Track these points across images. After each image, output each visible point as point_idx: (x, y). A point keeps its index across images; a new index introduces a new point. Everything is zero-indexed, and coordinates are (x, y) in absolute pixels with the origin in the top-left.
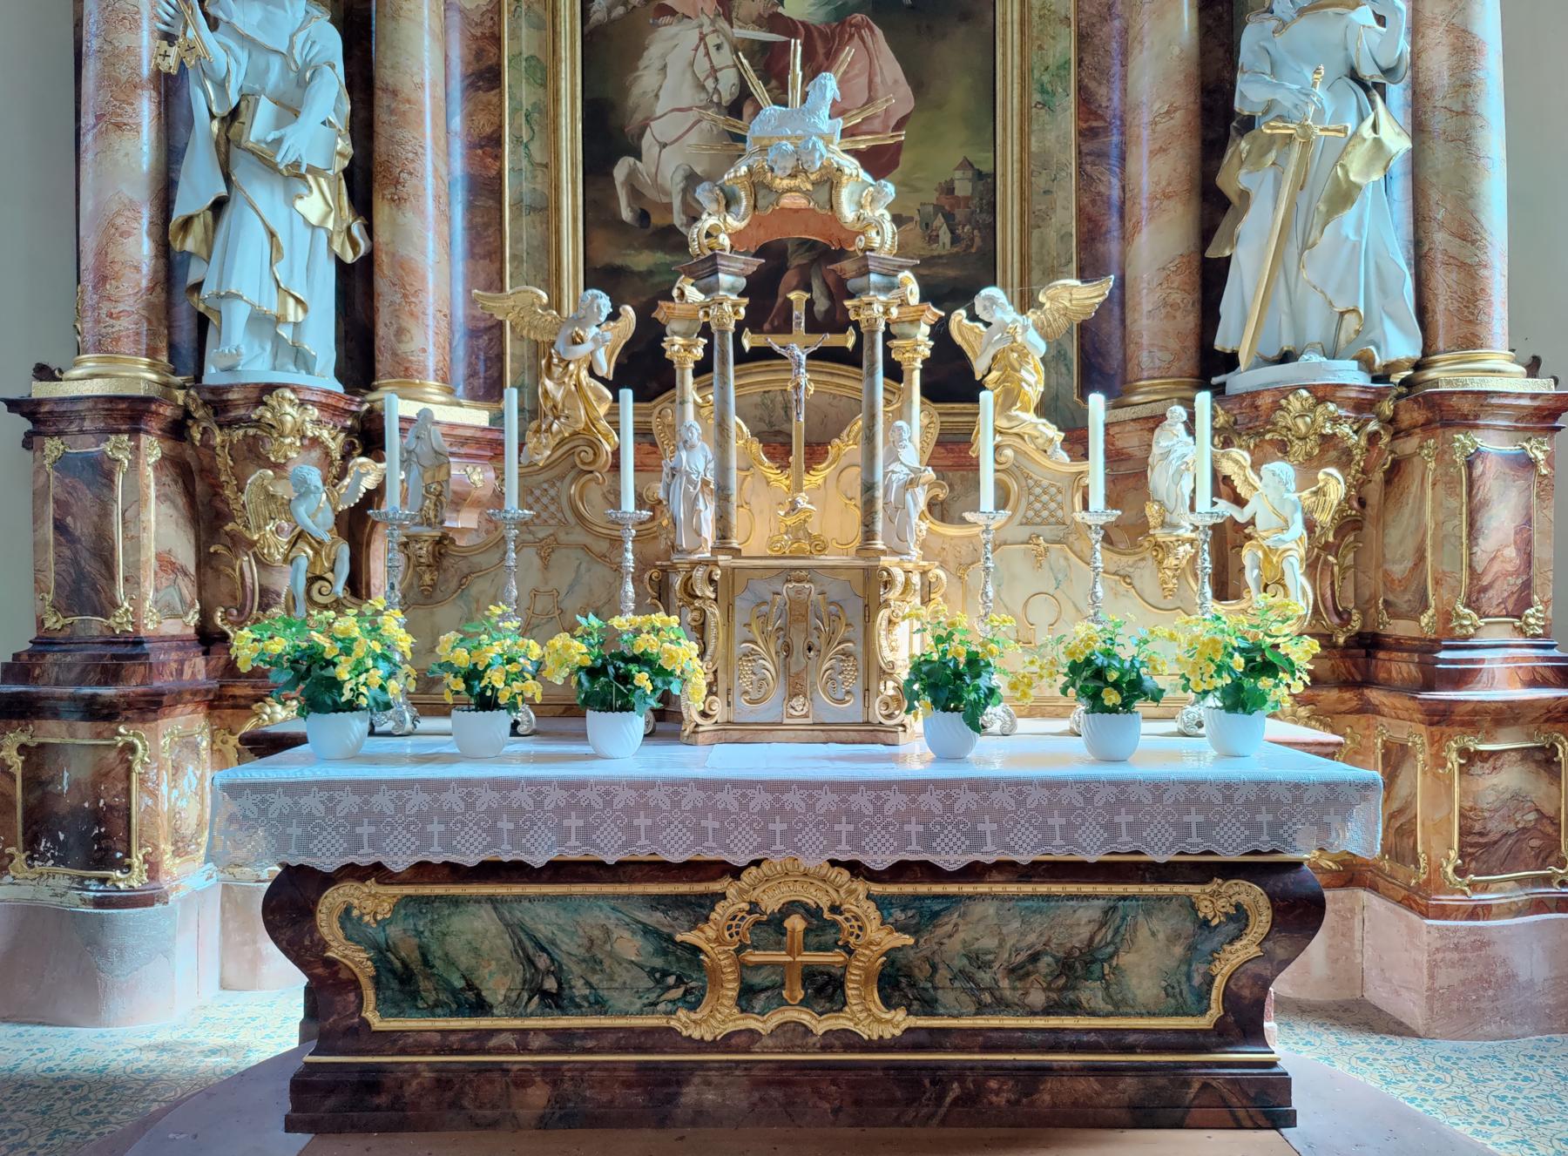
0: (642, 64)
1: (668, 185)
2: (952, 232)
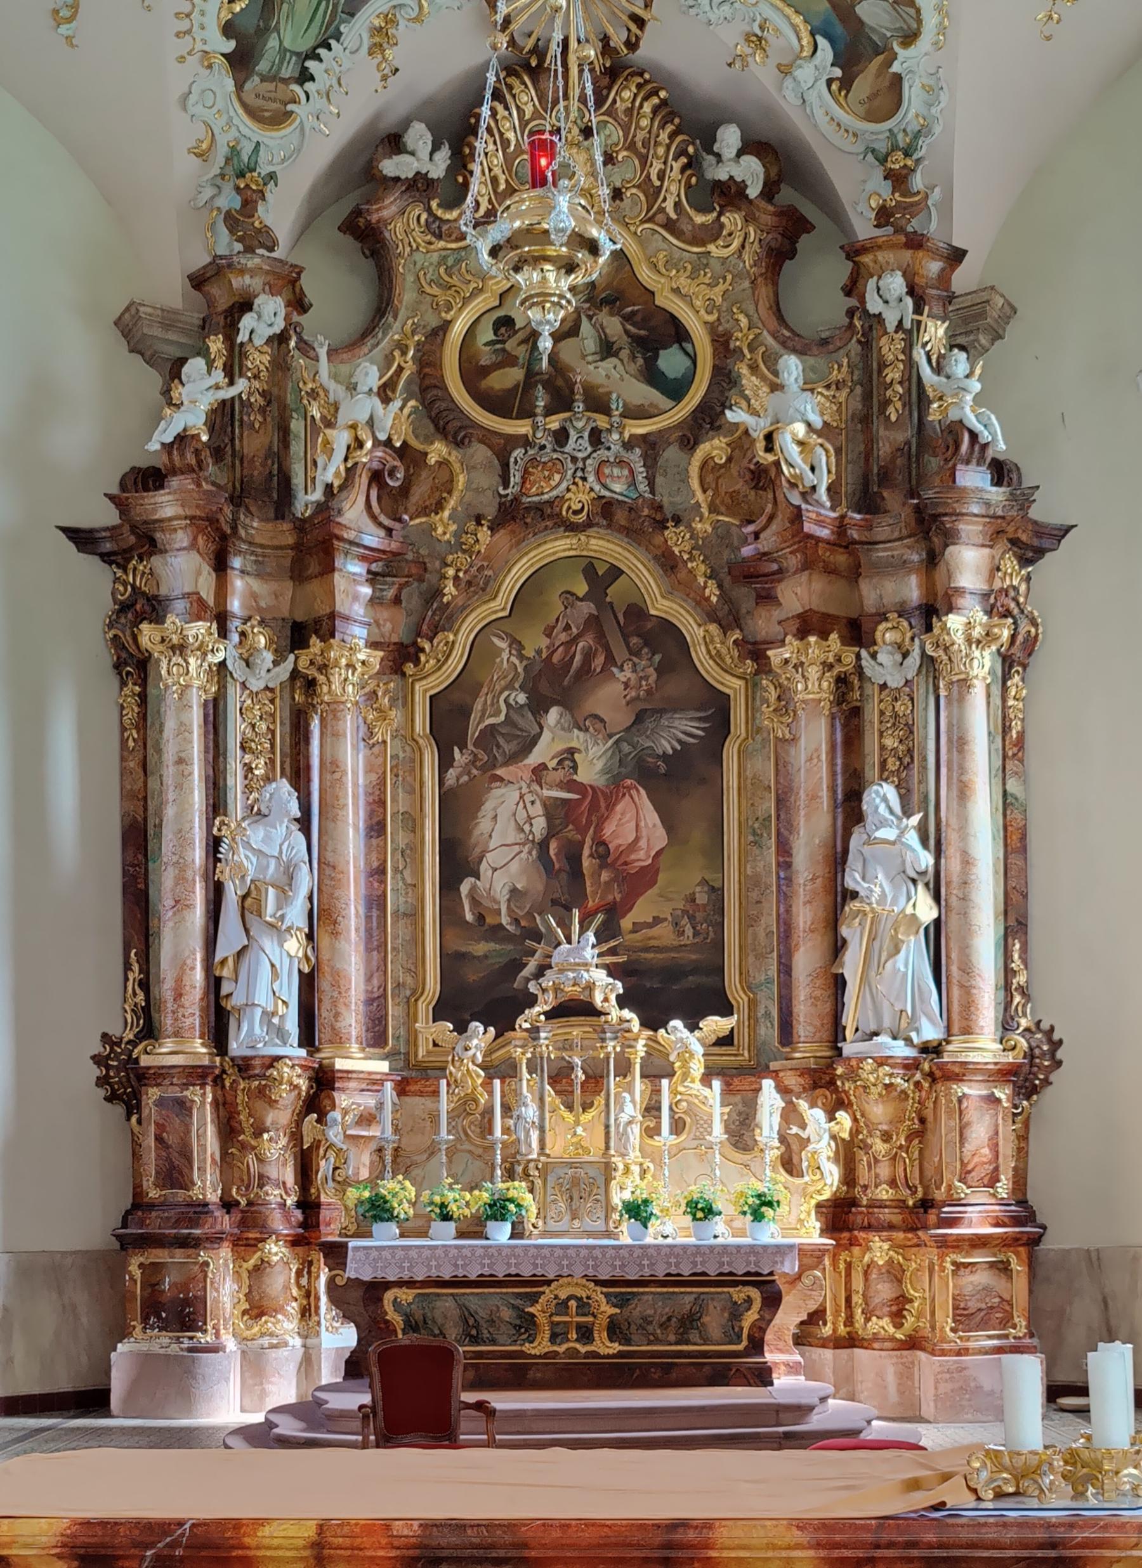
0: (480, 814)
1: (498, 896)
2: (694, 928)
